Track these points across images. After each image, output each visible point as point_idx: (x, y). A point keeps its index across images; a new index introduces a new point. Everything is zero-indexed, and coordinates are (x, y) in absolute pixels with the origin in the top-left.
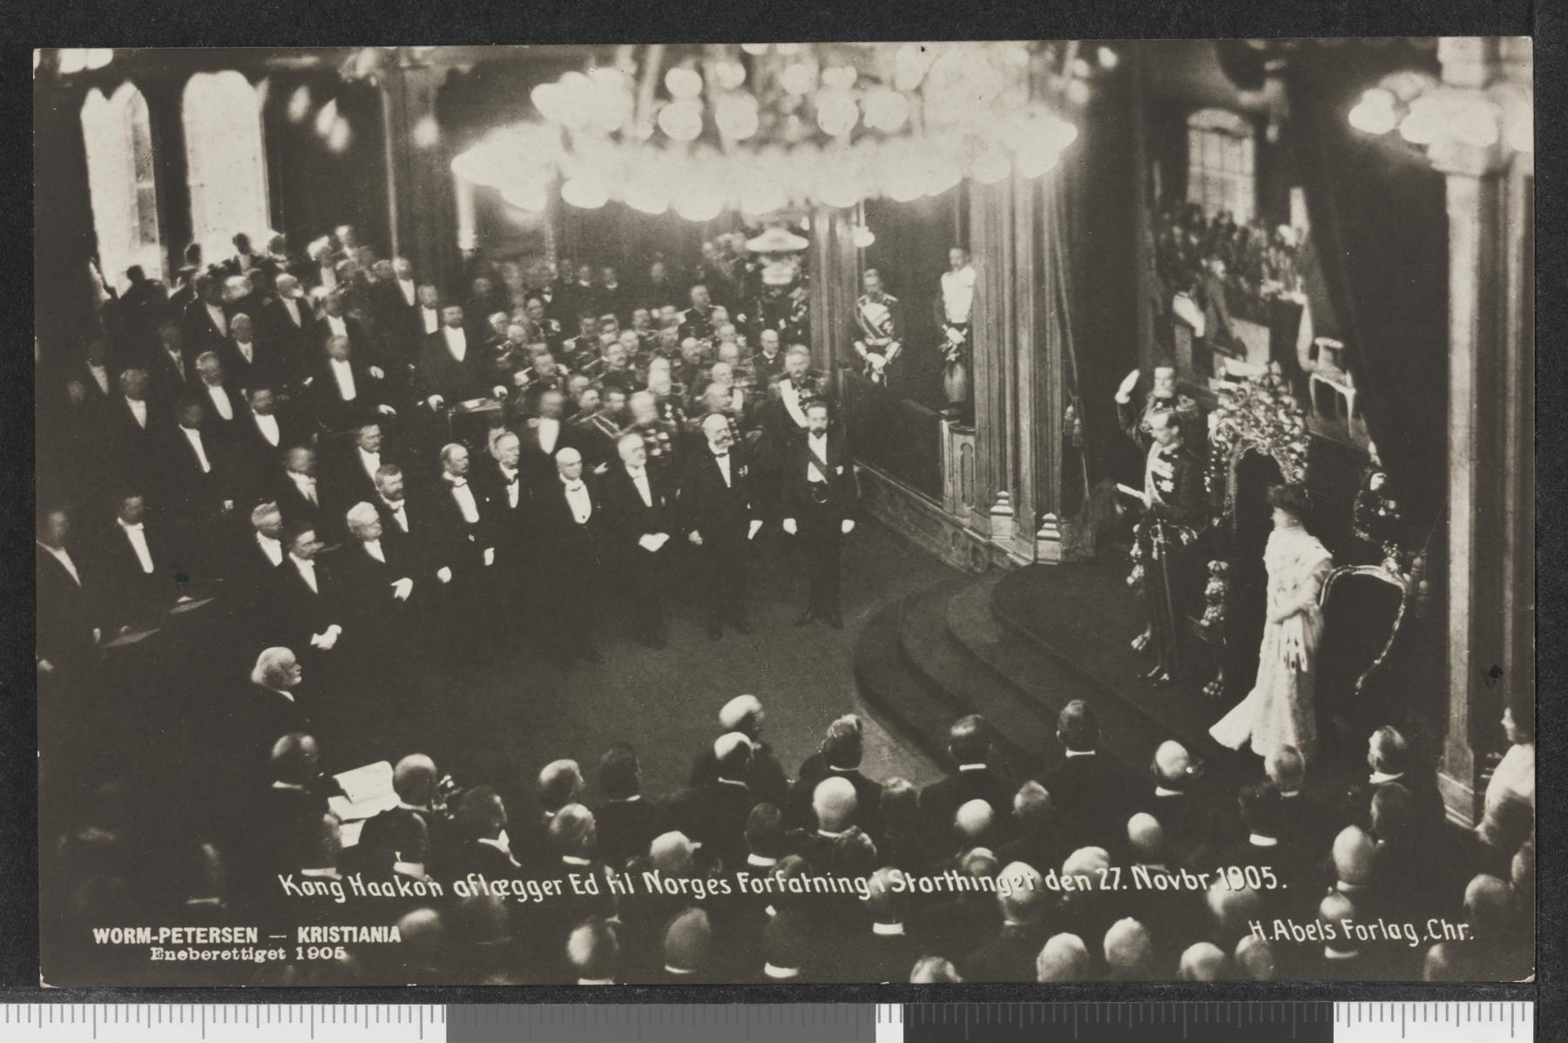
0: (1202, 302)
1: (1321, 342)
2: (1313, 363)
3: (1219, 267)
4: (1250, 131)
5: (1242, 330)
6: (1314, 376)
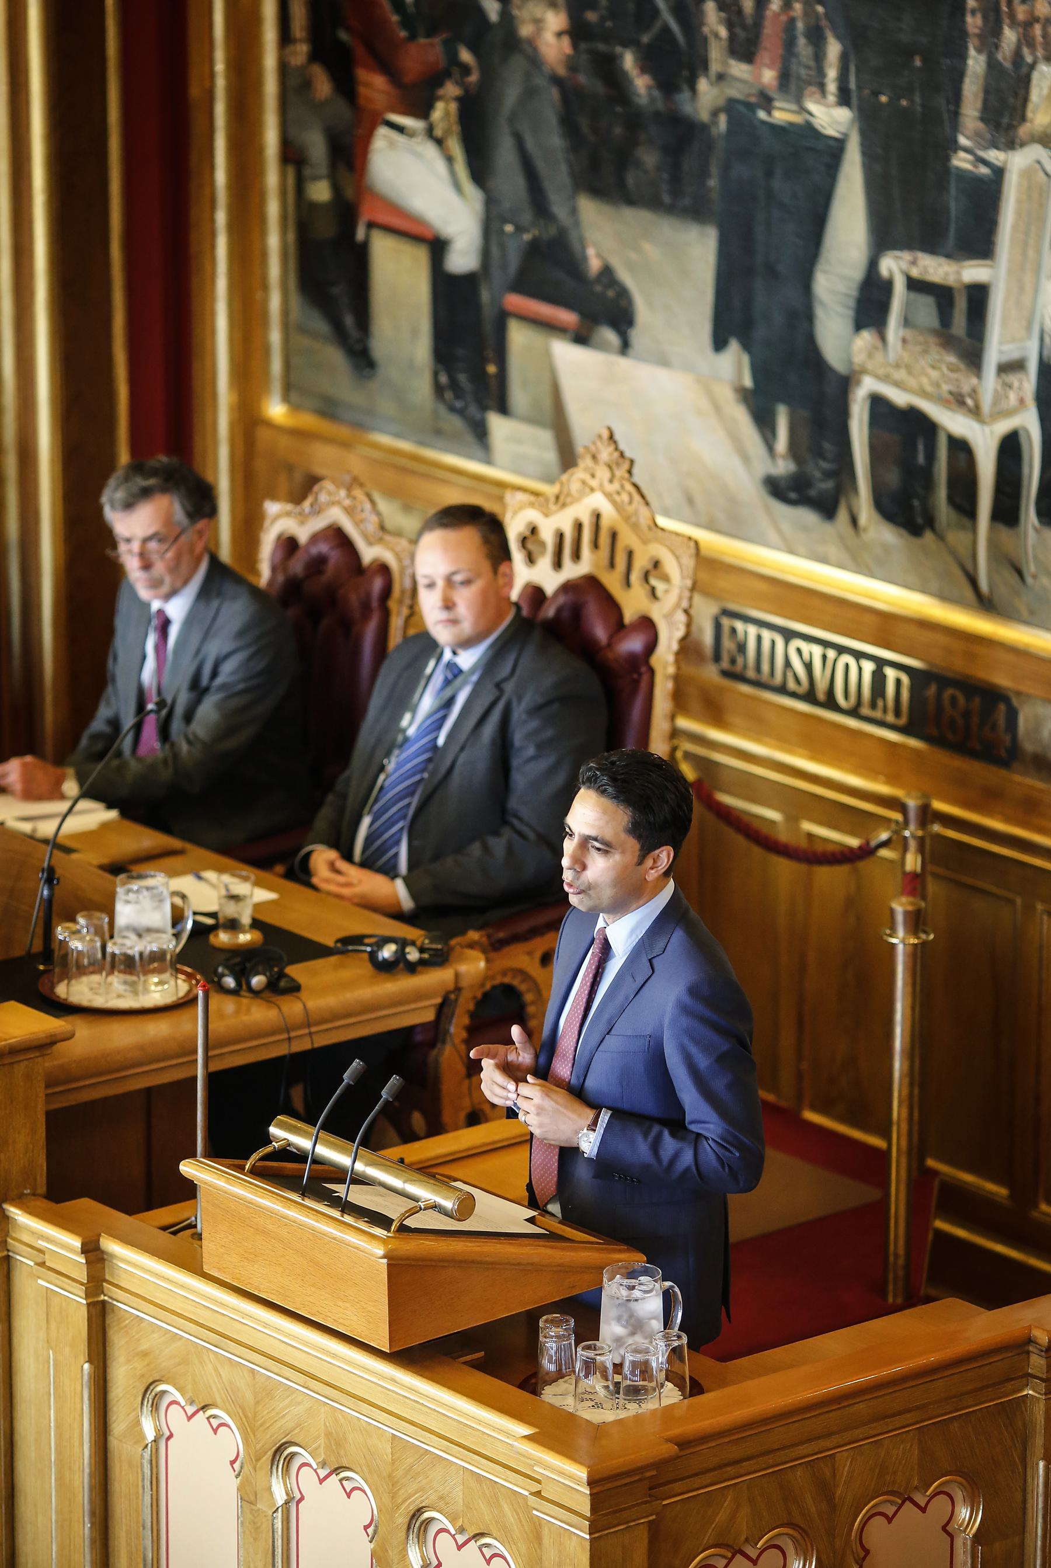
1: (892, 265)
2: (866, 337)
5: (607, 236)
6: (867, 385)
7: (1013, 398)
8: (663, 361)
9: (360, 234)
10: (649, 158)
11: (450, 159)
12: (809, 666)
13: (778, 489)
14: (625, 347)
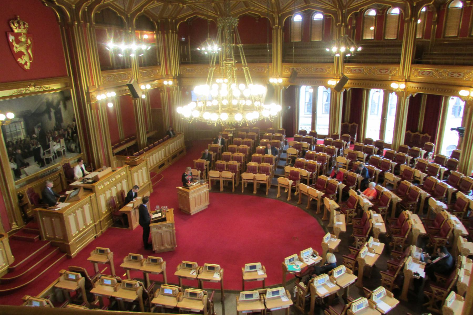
1: (45, 152)
3: (19, 151)
4: (22, 120)
5: (26, 161)
13: (41, 167)
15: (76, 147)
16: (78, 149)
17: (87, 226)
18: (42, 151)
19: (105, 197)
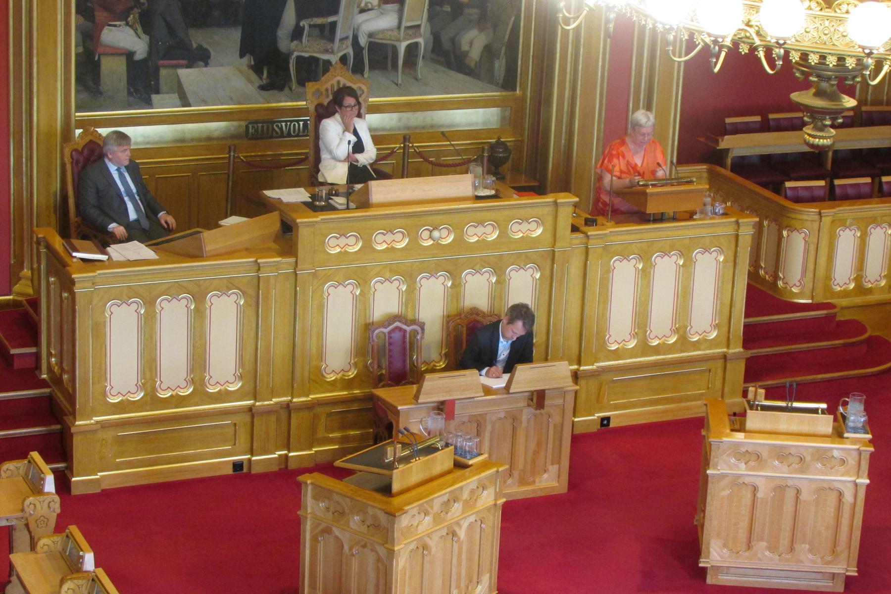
0: (146, 24)
7: (344, 46)
8: (222, 65)
9: (96, 58)
10: (216, 13)
11: (135, 30)
12: (281, 128)
13: (262, 88)
14: (206, 65)
15: (489, 51)
16: (500, 66)
17: (200, 394)
18: (289, 16)
19: (363, 302)
